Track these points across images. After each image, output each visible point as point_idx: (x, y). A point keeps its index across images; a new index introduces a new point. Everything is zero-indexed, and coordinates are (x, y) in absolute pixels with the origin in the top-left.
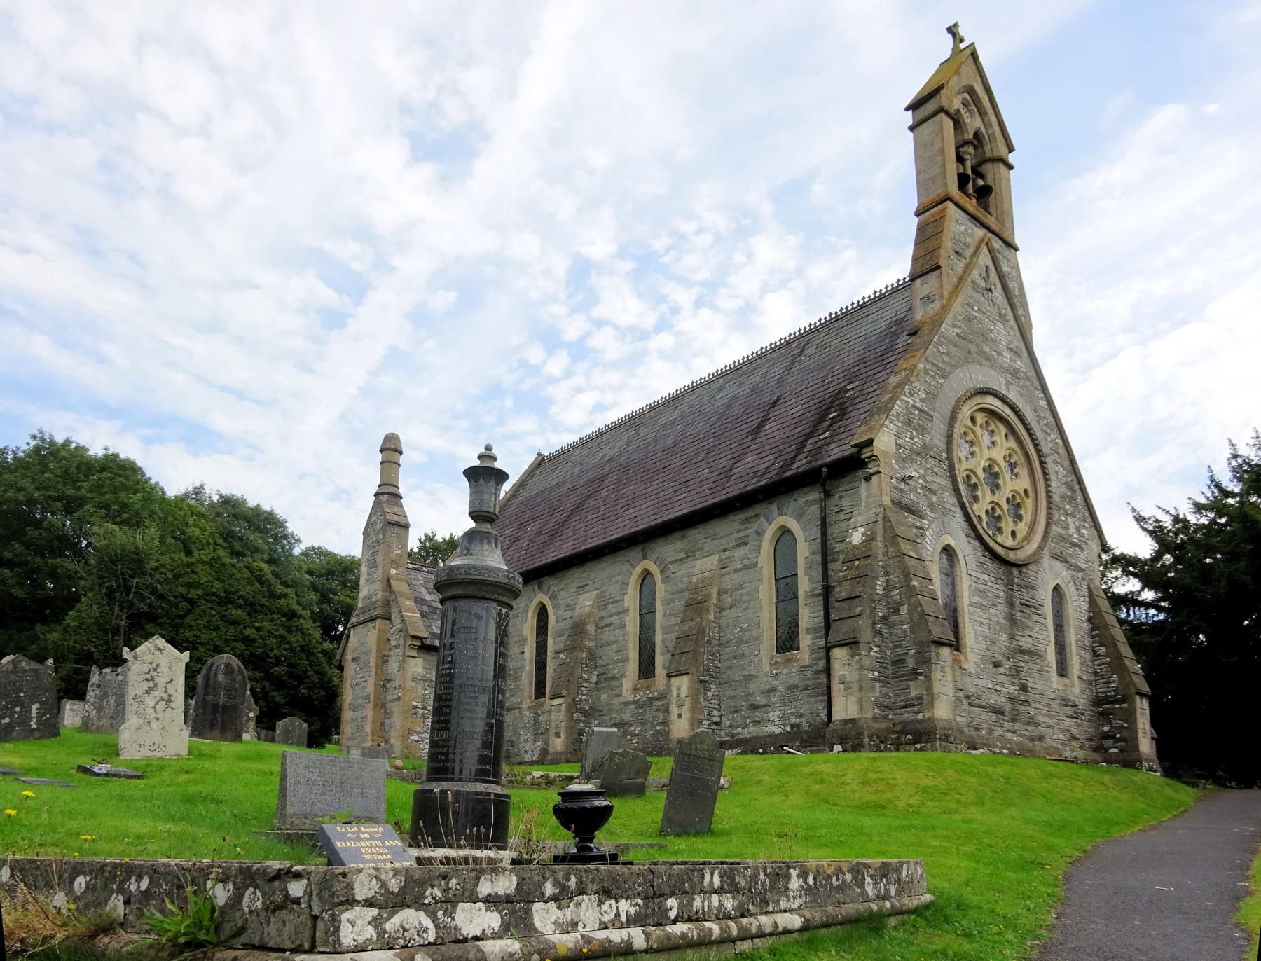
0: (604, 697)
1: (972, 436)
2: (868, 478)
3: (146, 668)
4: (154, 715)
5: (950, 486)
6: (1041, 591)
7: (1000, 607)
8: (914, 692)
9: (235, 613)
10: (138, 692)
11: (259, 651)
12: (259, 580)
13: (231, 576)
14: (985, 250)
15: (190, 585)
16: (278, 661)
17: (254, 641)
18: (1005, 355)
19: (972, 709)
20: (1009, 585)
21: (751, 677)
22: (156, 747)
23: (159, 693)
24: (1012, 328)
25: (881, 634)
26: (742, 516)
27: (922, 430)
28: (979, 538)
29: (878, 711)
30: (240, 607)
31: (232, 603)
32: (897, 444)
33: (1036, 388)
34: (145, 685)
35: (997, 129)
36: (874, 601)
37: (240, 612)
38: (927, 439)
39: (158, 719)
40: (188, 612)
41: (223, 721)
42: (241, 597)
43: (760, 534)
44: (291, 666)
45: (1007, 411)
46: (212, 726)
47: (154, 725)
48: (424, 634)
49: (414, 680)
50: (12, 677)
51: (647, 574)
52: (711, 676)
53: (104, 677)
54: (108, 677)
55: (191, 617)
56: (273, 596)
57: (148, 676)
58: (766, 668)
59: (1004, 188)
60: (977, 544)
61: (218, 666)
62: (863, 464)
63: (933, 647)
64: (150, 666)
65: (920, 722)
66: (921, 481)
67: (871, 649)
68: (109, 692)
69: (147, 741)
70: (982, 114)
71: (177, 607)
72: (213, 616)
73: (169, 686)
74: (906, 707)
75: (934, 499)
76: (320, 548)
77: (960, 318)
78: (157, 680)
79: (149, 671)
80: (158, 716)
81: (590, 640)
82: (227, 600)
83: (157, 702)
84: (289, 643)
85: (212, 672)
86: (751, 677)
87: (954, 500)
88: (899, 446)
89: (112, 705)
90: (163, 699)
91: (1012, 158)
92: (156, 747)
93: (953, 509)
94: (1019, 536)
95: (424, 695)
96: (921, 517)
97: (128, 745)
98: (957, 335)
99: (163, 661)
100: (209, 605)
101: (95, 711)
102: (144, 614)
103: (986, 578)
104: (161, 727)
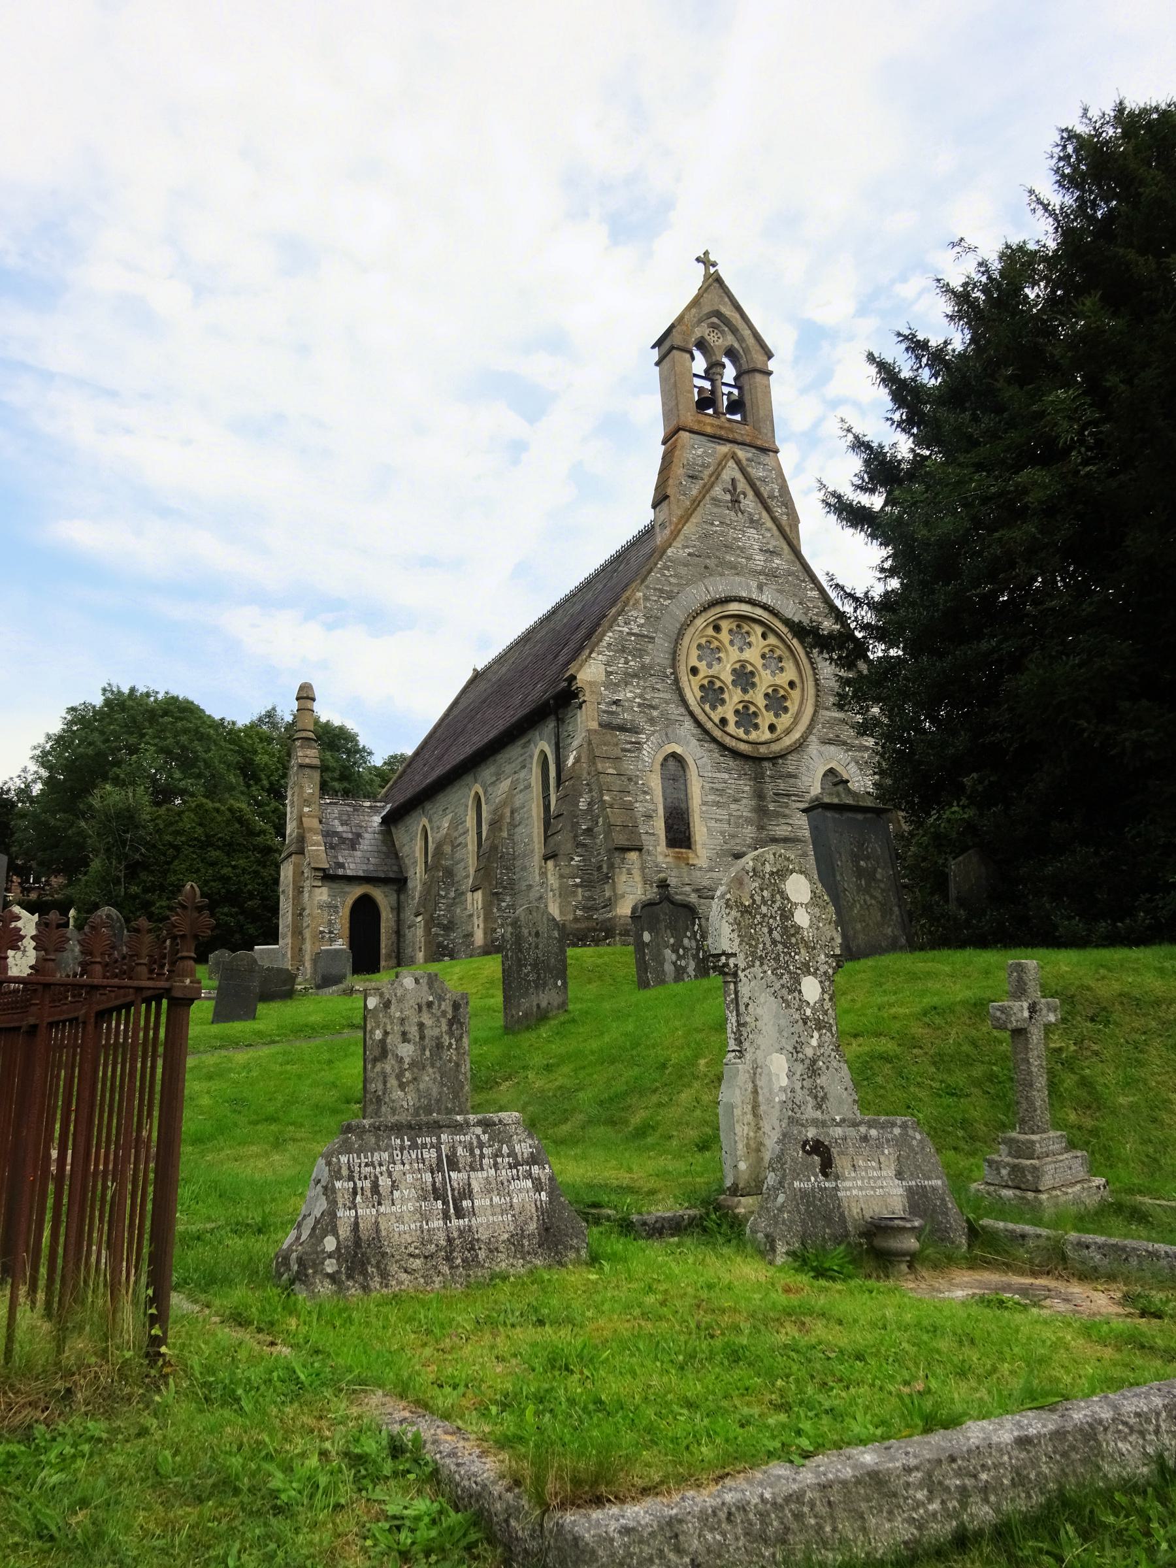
0: (458, 911)
1: (716, 643)
2: (580, 707)
5: (676, 697)
6: (804, 778)
7: (744, 801)
8: (607, 894)
9: (214, 854)
11: (233, 888)
12: (240, 820)
13: (212, 820)
14: (731, 463)
15: (177, 833)
16: (251, 896)
17: (229, 878)
18: (757, 558)
19: (702, 901)
20: (758, 778)
21: (530, 887)
24: (768, 530)
25: (584, 845)
26: (523, 741)
27: (640, 653)
28: (714, 740)
29: (579, 913)
30: (219, 848)
31: (212, 845)
32: (607, 672)
33: (804, 581)
35: (751, 341)
36: (576, 817)
37: (218, 853)
38: (647, 660)
40: (175, 857)
42: (220, 839)
43: (531, 757)
44: (263, 899)
45: (759, 612)
48: (327, 866)
49: (320, 907)
51: (477, 796)
52: (505, 888)
55: (176, 862)
56: (252, 833)
58: (538, 878)
59: (760, 395)
60: (713, 746)
62: (575, 695)
63: (616, 854)
65: (610, 919)
66: (637, 700)
67: (572, 859)
70: (734, 331)
71: (164, 855)
72: (194, 859)
74: (604, 907)
75: (655, 713)
76: (402, 755)
77: (693, 538)
81: (446, 859)
82: (207, 843)
84: (262, 878)
86: (530, 887)
87: (682, 710)
88: (609, 674)
91: (772, 365)
93: (681, 718)
94: (780, 729)
95: (330, 920)
96: (637, 733)
98: (689, 554)
100: (191, 849)
102: (138, 863)
103: (726, 776)
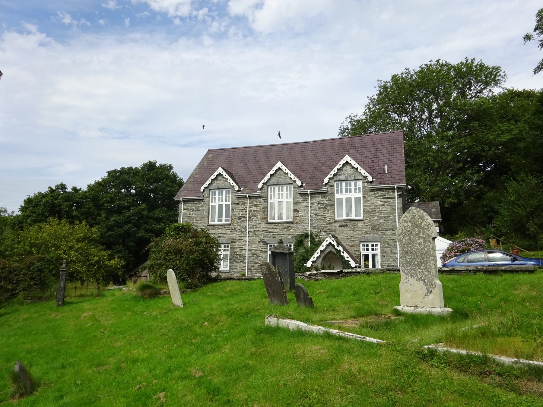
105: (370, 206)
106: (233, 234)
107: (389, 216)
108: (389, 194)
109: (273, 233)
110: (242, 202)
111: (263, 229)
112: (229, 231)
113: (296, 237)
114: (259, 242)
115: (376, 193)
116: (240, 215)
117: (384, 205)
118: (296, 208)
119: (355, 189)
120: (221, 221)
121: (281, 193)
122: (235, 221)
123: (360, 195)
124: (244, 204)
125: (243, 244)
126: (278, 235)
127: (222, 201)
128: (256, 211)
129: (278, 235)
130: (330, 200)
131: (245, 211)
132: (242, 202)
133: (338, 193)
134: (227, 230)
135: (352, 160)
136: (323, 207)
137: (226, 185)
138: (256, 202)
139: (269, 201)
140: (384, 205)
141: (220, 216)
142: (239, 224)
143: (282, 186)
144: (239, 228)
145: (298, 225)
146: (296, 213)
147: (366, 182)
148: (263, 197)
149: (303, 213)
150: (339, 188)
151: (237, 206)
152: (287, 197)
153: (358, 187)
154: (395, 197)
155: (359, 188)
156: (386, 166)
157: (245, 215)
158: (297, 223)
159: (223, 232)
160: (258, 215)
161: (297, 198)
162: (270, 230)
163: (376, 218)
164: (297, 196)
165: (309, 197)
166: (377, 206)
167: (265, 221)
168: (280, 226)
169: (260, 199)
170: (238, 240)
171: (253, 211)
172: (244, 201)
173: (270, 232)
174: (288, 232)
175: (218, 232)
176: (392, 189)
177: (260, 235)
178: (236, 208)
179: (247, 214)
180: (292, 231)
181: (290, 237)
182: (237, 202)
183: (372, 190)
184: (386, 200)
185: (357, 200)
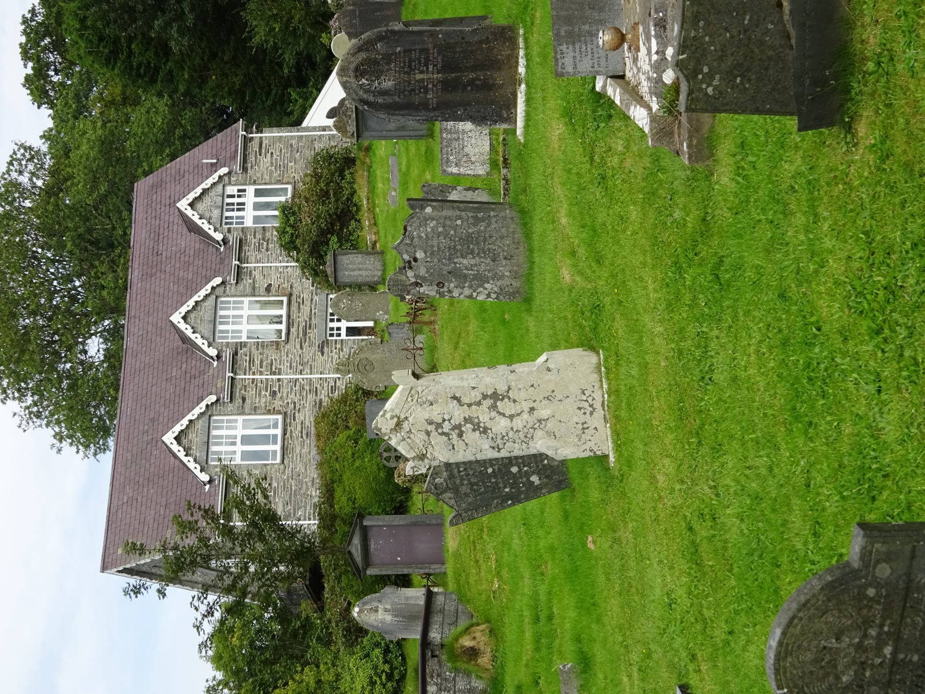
3: (436, 439)
4: (525, 416)
10: (486, 444)
22: (586, 405)
23: (483, 414)
34: (471, 436)
39: (532, 409)
41: (474, 68)
46: (488, 86)
47: (543, 413)
50: (464, 489)
53: (424, 279)
54: (422, 271)
57: (454, 435)
61: (366, 91)
64: (434, 434)
68: (450, 268)
69: (575, 419)
73: (465, 400)
78: (458, 418)
79: (443, 434)
80: (526, 409)
83: (499, 413)
85: (380, 100)
89: (473, 262)
90: (494, 407)
92: (586, 405)
97: (584, 447)
99: (419, 415)
101: (486, 285)
104: (546, 402)
105: (271, 173)
106: (304, 407)
107: (291, 145)
108: (255, 146)
109: (308, 326)
110: (241, 390)
111: (298, 347)
112: (297, 414)
113: (317, 288)
114: (323, 355)
115: (249, 165)
116: (268, 394)
117: (272, 153)
118: (262, 290)
119: (239, 196)
120: (275, 436)
121: (231, 320)
122: (277, 403)
123: (251, 190)
124: (245, 387)
125: (326, 385)
126: (310, 319)
127: (241, 317)
128: (262, 362)
129: (310, 319)
130: (255, 232)
131: (259, 384)
132: (241, 390)
133: (243, 223)
134: (294, 420)
135: (173, 429)
136: (265, 243)
137: (203, 426)
138: (243, 361)
139: (244, 339)
140: (272, 153)
141: (265, 439)
142: (285, 395)
143: (218, 317)
144: (293, 396)
145: (295, 285)
146: (273, 290)
147: (229, 178)
148: (236, 349)
149: (274, 277)
150: (224, 440)
151: (248, 401)
152: (235, 428)
153: (236, 193)
154: (261, 138)
155: (239, 191)
156: (205, 161)
157: (267, 384)
158: (291, 287)
159: (299, 428)
160: (270, 358)
161: (245, 286)
162: (301, 335)
163: (292, 164)
164: (240, 287)
165: (246, 265)
166: (272, 163)
167: (283, 344)
168: (294, 316)
169: (239, 355)
170: (316, 395)
171: (261, 367)
172: (239, 387)
173: (305, 334)
174: (307, 303)
175: (297, 438)
176: (246, 140)
177: (309, 352)
178: (252, 402)
179: (267, 379)
180: (305, 295)
181: (316, 298)
182: (241, 401)
183: (245, 169)
184: (263, 151)
185: (258, 193)
